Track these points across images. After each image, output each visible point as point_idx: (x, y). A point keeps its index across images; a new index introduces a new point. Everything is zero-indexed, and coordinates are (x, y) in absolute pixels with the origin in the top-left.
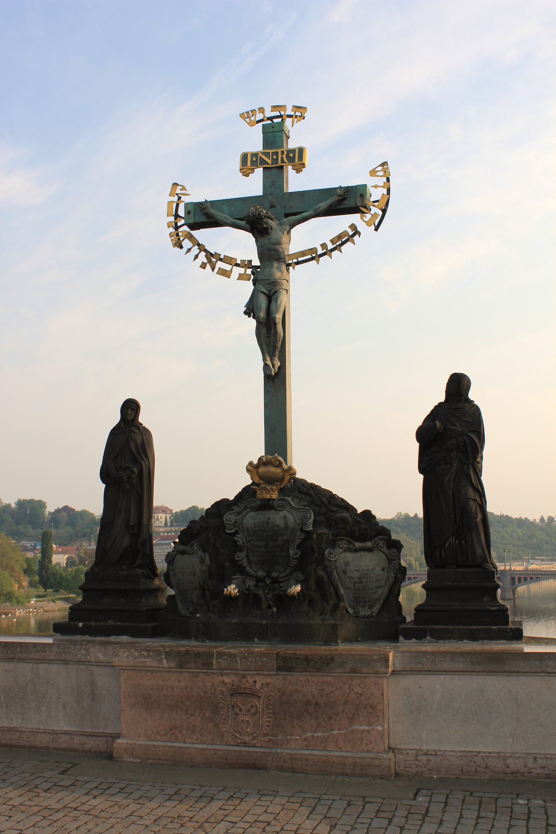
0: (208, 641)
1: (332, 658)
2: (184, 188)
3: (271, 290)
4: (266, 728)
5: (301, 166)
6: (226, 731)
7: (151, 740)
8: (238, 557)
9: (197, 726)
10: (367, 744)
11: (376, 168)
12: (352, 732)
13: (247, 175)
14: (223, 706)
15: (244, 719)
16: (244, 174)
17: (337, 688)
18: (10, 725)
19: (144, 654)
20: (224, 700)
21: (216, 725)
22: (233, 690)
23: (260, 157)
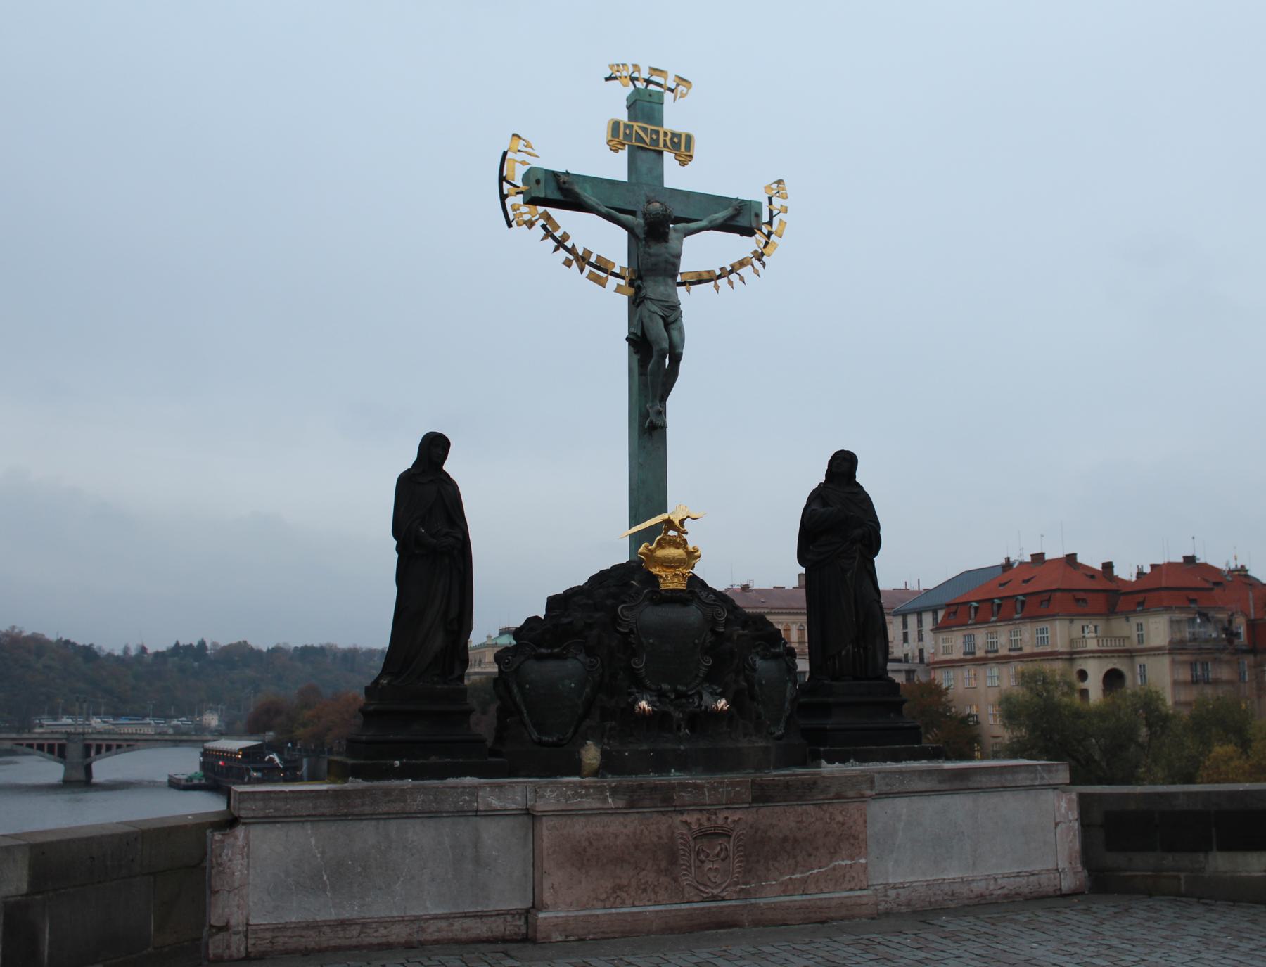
0: (610, 776)
1: (815, 783)
2: (528, 145)
4: (737, 875)
5: (688, 158)
6: (687, 884)
8: (636, 665)
9: (649, 883)
10: (849, 881)
12: (834, 869)
13: (616, 151)
14: (683, 853)
15: (711, 866)
16: (614, 148)
17: (817, 819)
18: (341, 917)
20: (685, 845)
21: (675, 880)
23: (636, 131)
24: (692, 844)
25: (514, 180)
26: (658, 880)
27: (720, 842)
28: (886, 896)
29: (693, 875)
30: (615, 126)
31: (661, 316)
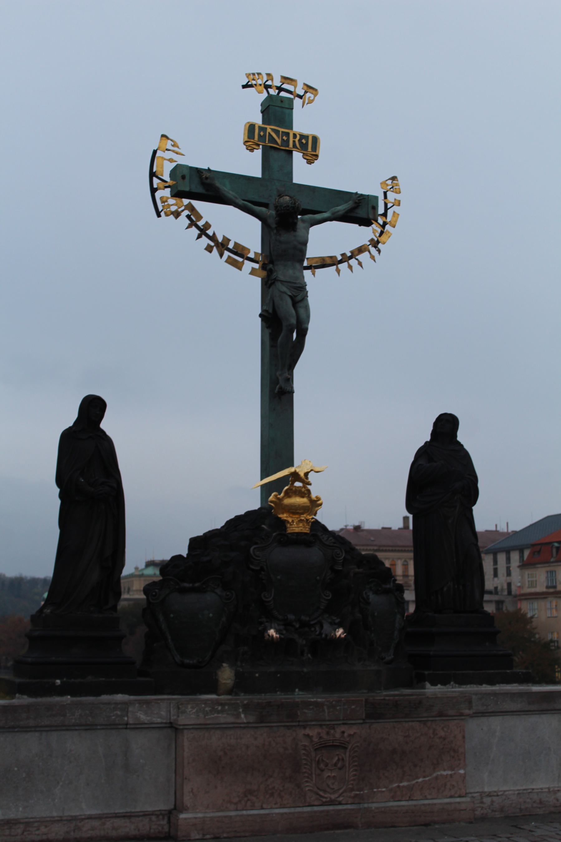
0: (242, 694)
2: (175, 145)
3: (297, 296)
4: (352, 782)
5: (314, 157)
6: (309, 790)
7: (222, 811)
10: (450, 789)
11: (387, 180)
12: (437, 778)
13: (252, 150)
14: (305, 762)
15: (330, 774)
16: (249, 148)
18: (7, 817)
19: (217, 708)
22: (320, 743)
23: (269, 133)
24: (313, 754)
25: (162, 175)
26: (283, 786)
27: (338, 753)
28: (482, 802)
29: (314, 781)
30: (251, 128)
31: (290, 296)
